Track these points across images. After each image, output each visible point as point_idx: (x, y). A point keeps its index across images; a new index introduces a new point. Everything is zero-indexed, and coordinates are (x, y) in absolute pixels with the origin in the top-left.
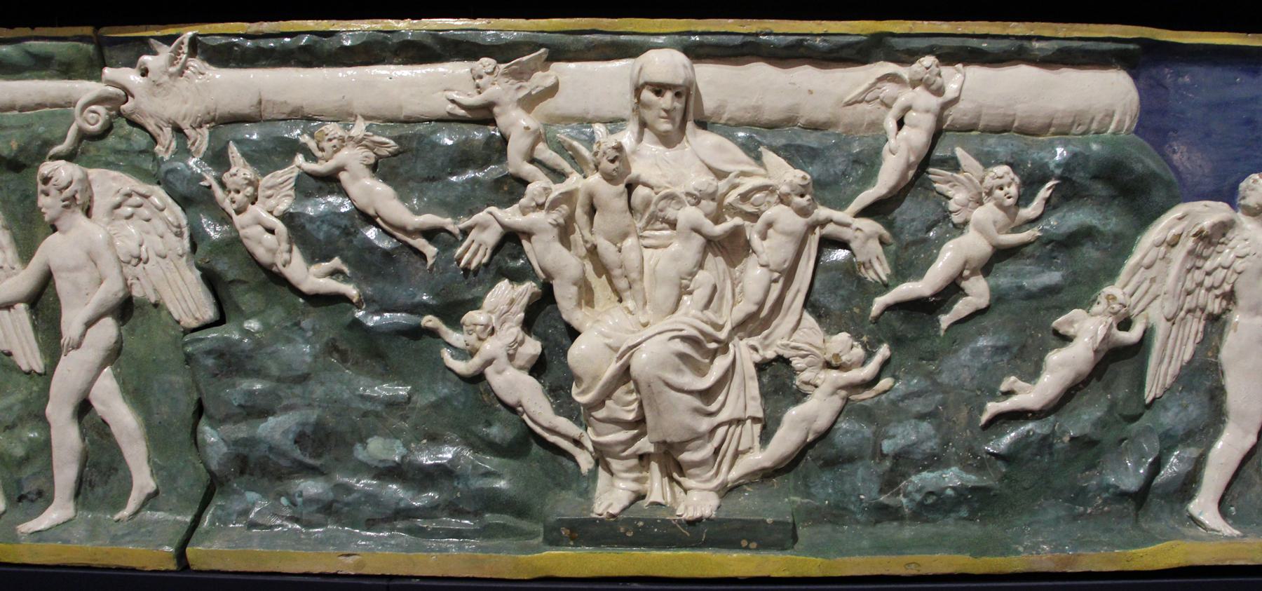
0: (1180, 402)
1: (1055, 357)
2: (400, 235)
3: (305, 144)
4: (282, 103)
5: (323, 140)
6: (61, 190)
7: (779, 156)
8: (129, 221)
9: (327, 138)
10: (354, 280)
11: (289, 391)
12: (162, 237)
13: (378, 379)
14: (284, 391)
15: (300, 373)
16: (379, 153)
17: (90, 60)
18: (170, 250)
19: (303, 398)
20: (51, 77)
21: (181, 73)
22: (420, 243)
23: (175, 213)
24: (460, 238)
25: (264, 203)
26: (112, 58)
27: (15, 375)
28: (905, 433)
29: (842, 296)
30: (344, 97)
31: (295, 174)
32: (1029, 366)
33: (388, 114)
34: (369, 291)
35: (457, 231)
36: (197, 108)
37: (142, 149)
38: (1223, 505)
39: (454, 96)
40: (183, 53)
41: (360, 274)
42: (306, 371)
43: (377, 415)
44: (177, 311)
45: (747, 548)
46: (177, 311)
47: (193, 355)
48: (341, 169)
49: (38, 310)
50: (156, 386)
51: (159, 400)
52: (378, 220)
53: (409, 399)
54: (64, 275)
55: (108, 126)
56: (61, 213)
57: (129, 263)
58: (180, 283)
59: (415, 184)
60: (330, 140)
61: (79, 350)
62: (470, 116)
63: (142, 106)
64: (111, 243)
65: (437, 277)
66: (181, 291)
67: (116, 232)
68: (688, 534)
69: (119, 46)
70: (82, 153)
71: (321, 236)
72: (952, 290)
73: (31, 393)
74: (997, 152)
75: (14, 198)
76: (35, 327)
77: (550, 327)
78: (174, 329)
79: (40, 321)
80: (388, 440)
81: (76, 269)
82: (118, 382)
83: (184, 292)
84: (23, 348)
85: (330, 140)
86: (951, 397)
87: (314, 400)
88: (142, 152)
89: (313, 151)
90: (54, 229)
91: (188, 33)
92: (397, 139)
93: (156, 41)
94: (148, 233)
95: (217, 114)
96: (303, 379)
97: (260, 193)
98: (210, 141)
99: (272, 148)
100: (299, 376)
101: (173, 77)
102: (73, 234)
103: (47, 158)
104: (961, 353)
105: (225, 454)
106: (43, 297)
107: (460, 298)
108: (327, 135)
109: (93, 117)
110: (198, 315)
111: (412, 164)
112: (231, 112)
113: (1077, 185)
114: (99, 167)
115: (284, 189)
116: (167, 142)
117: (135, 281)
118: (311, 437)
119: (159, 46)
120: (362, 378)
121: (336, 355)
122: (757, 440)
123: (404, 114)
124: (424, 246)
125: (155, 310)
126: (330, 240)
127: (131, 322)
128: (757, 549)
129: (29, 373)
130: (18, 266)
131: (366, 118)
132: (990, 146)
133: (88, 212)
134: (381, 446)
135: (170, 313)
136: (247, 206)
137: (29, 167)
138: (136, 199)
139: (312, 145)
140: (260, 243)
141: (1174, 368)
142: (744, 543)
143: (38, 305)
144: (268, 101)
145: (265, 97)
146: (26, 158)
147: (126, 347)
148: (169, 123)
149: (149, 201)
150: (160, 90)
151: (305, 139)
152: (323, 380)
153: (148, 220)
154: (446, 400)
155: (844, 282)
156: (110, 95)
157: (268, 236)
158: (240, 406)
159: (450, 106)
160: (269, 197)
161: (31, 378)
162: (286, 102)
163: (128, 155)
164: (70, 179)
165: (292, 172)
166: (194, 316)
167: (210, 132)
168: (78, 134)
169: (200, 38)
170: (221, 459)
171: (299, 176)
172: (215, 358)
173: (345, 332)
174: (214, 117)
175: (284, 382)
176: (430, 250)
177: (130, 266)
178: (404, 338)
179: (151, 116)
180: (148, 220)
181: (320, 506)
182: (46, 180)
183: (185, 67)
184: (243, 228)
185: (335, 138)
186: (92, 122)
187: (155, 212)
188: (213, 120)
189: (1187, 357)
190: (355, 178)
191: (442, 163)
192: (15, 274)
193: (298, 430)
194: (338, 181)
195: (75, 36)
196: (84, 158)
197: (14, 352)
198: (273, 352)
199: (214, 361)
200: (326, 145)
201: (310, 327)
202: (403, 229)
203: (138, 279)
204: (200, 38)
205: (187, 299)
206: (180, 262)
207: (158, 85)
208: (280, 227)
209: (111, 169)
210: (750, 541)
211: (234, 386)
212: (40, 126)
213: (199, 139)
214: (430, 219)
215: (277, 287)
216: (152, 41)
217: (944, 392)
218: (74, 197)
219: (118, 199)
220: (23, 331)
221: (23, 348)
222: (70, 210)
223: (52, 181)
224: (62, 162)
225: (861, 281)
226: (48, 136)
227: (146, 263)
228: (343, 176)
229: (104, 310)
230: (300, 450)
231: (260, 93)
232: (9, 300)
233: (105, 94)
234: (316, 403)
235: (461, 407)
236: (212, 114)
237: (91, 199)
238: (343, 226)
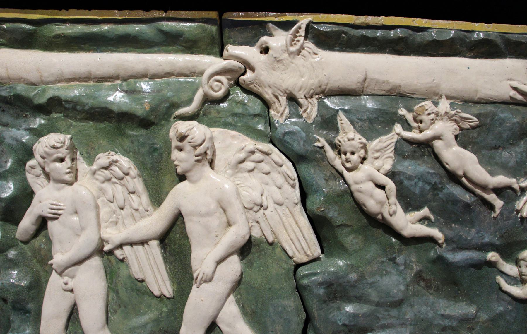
2: (479, 191)
3: (404, 116)
4: (384, 82)
5: (423, 113)
6: (195, 147)
8: (251, 174)
9: (427, 112)
10: (437, 224)
11: (386, 313)
12: (280, 188)
13: (452, 300)
14: (382, 313)
15: (396, 299)
16: (463, 126)
17: (213, 38)
18: (287, 199)
19: (398, 318)
20: (176, 52)
21: (299, 52)
22: (492, 197)
23: (288, 167)
24: (519, 194)
25: (372, 163)
26: (230, 38)
27: (147, 298)
30: (433, 80)
31: (395, 140)
33: (466, 96)
34: (450, 234)
35: (518, 189)
36: (311, 82)
37: (257, 113)
39: (515, 84)
40: (300, 36)
41: (442, 220)
42: (401, 297)
43: (453, 329)
44: (292, 249)
46: (292, 249)
47: (309, 286)
48: (438, 137)
49: (166, 245)
50: (271, 309)
51: (274, 321)
52: (464, 179)
53: (475, 317)
54: (195, 219)
55: (227, 93)
56: (194, 166)
57: (251, 209)
58: (295, 226)
59: (487, 151)
60: (429, 114)
61: (210, 283)
62: (525, 101)
63: (262, 78)
64: (238, 194)
65: (501, 223)
66: (295, 233)
67: (239, 182)
69: (239, 28)
70: (204, 114)
71: (417, 191)
73: (161, 314)
75: (144, 150)
76: (165, 259)
78: (286, 262)
79: (168, 254)
81: (208, 214)
82: (239, 305)
83: (297, 234)
84: (155, 276)
85: (429, 114)
87: (407, 320)
88: (256, 115)
89: (410, 122)
90: (182, 178)
92: (478, 116)
93: (274, 26)
94: (267, 184)
95: (328, 87)
96: (398, 304)
97: (370, 155)
98: (318, 110)
99: (375, 118)
100: (396, 302)
101: (292, 56)
102: (202, 184)
103: (173, 117)
106: (170, 234)
107: (518, 239)
108: (427, 110)
109: (217, 85)
110: (309, 253)
111: (485, 136)
112: (341, 86)
114: (218, 126)
115: (387, 152)
116: (282, 109)
117: (255, 224)
119: (275, 29)
120: (441, 301)
121: (422, 284)
123: (478, 96)
124: (495, 200)
125: (270, 247)
126: (423, 193)
127: (250, 256)
129: (161, 298)
130: (150, 208)
131: (448, 98)
133: (211, 163)
135: (284, 250)
136: (358, 165)
137: (157, 124)
138: (258, 156)
139: (409, 117)
140: (371, 196)
143: (166, 241)
144: (372, 79)
145: (372, 75)
146: (156, 117)
147: (245, 278)
148: (286, 93)
149: (270, 157)
150: (279, 66)
151: (402, 112)
152: (412, 304)
153: (267, 174)
154: (501, 315)
156: (233, 68)
157: (379, 191)
158: (344, 325)
159: (513, 93)
160: (377, 158)
161: (160, 301)
162: (387, 81)
163: (243, 117)
164: (204, 138)
165: (393, 138)
166: (305, 253)
167: (318, 102)
168: (203, 99)
169: (315, 26)
171: (397, 142)
172: (324, 288)
173: (429, 266)
174: (325, 90)
175: (381, 306)
176: (498, 203)
177: (251, 212)
178: (472, 269)
179: (270, 87)
180: (267, 174)
182: (182, 138)
183: (302, 48)
184: (357, 183)
185: (433, 113)
186: (216, 89)
187: (274, 167)
188: (323, 92)
190: (449, 146)
191: (507, 136)
192: (149, 215)
194: (432, 147)
195: (202, 19)
196: (206, 119)
197: (147, 280)
198: (373, 283)
199: (324, 290)
200: (424, 117)
201: (403, 263)
202: (484, 188)
203: (257, 222)
204: (315, 26)
205: (300, 239)
206: (295, 209)
207: (278, 61)
208: (390, 184)
209: (229, 128)
211: (339, 309)
212: (168, 92)
213: (310, 108)
214: (501, 180)
215: (374, 230)
216: (270, 25)
218: (206, 153)
219: (242, 155)
220: (155, 262)
221: (155, 276)
222: (200, 164)
223: (189, 139)
224: (194, 123)
226: (176, 100)
227: (265, 209)
228: (438, 144)
229: (234, 250)
231: (366, 75)
232: (145, 238)
233: (229, 67)
234: (409, 322)
235: (513, 321)
236: (323, 87)
237: (214, 154)
238: (433, 183)
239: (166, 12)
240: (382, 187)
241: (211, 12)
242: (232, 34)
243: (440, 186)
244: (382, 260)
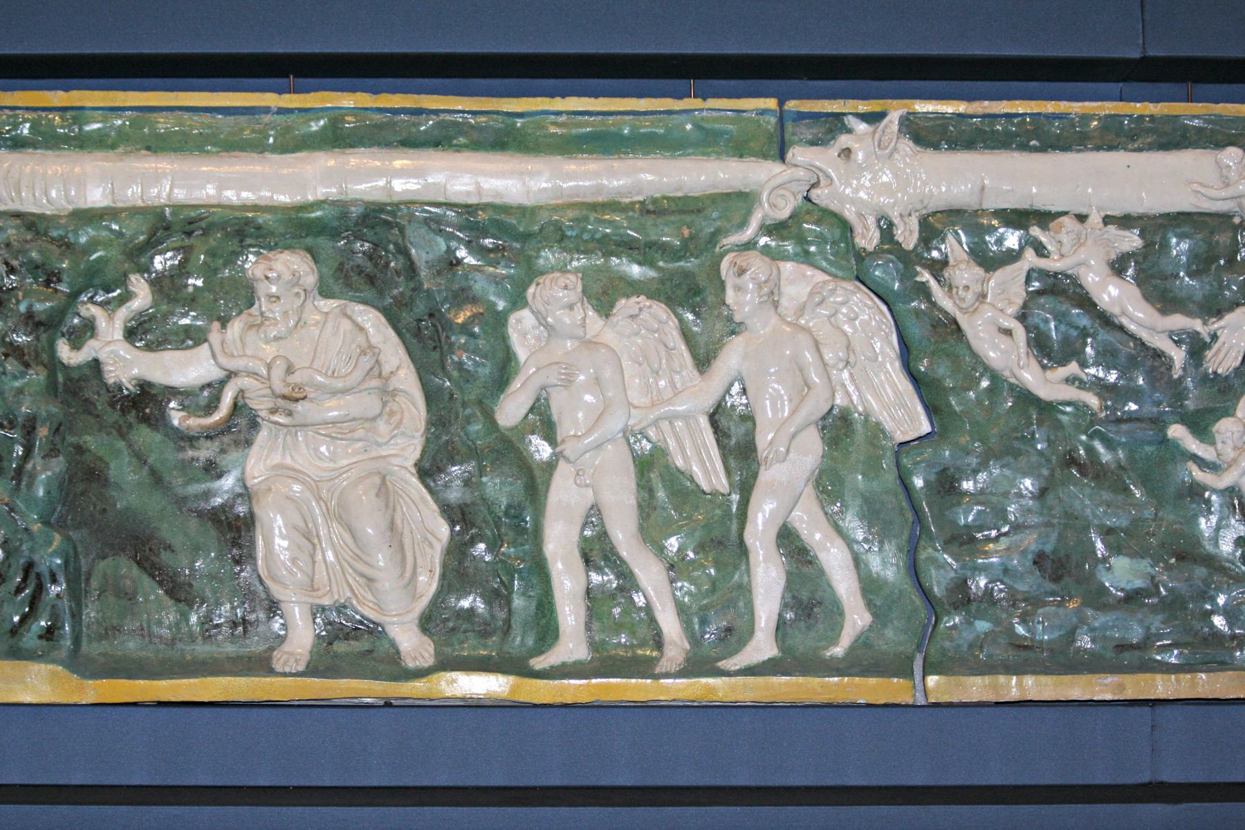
26: (794, 134)
80: (1134, 560)
91: (896, 111)
105: (952, 579)
134: (1127, 566)
176: (1178, 356)
181: (1062, 633)
216: (850, 117)
236: (926, 202)
239: (704, 99)
240: (1008, 332)
241: (768, 100)
242: (797, 129)
243: (1092, 331)
244: (1016, 435)
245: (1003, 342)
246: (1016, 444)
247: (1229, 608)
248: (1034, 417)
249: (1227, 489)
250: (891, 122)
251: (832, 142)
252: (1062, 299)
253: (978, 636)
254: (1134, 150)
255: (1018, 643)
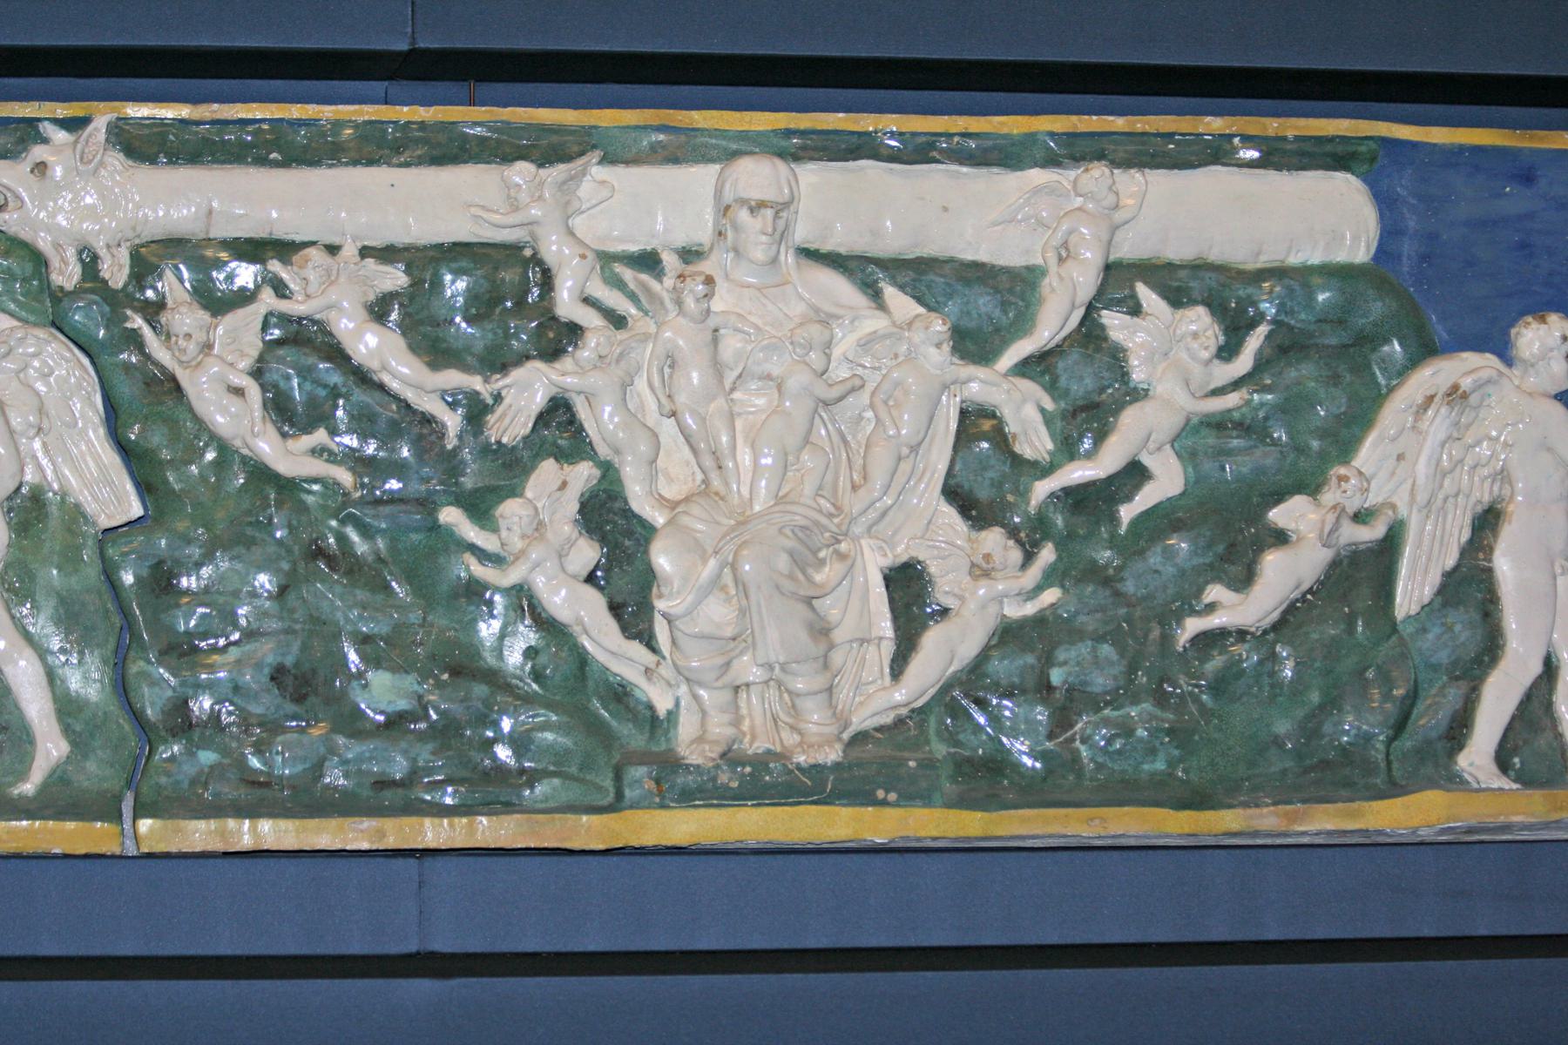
0: (1444, 620)
1: (1272, 562)
7: (906, 294)
28: (1080, 659)
29: (992, 479)
32: (1235, 570)
38: (1502, 760)
45: (884, 803)
68: (809, 783)
72: (1135, 473)
74: (1191, 288)
77: (608, 522)
80: (397, 676)
86: (1138, 613)
91: (103, 117)
104: (1149, 553)
113: (1296, 330)
118: (293, 671)
122: (887, 670)
128: (896, 805)
132: (1180, 280)
134: (388, 683)
141: (1434, 579)
142: (880, 794)
155: (993, 462)
170: (164, 705)
176: (453, 422)
181: (307, 766)
189: (1451, 562)
193: (275, 664)
210: (887, 791)
216: (46, 123)
217: (1128, 606)
225: (1017, 461)
230: (278, 689)
236: (139, 229)
238: (332, 385)
240: (239, 392)
244: (250, 519)
245: (234, 404)
246: (249, 531)
247: (516, 736)
248: (272, 496)
249: (513, 587)
250: (96, 129)
251: (23, 155)
252: (307, 351)
253: (202, 771)
254: (400, 165)
255: (250, 779)
